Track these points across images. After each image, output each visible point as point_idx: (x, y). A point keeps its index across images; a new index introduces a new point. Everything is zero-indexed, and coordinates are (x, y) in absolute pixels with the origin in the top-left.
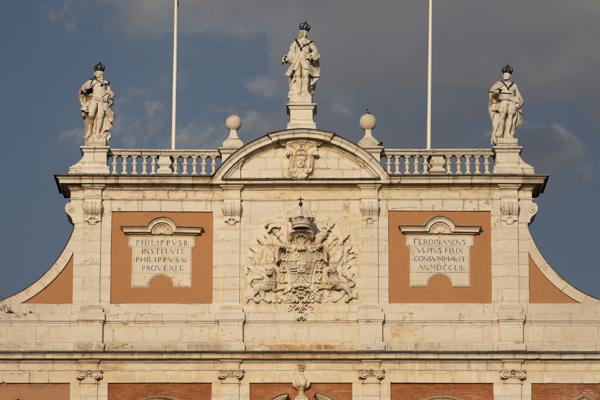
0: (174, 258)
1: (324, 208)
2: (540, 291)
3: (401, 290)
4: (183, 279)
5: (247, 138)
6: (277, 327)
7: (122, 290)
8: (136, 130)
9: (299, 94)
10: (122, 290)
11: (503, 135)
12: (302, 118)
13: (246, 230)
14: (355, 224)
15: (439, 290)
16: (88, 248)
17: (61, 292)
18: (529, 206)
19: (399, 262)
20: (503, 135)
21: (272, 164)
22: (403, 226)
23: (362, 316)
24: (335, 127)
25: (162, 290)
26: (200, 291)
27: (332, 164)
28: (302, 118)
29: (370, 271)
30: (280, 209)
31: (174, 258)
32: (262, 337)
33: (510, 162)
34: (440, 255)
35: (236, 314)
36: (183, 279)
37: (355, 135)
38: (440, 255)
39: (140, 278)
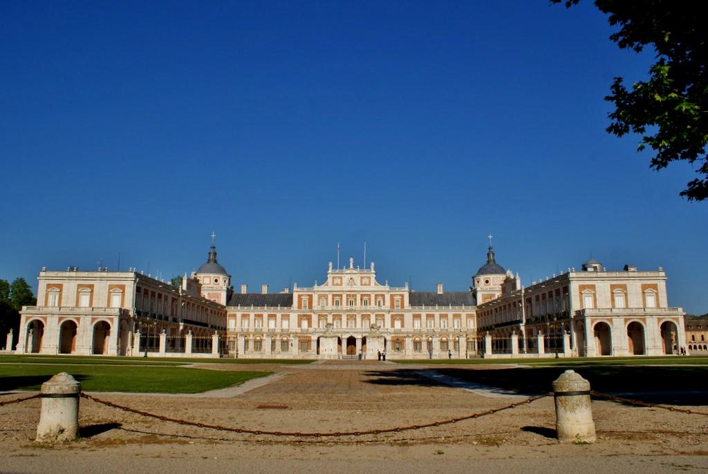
0: (338, 281)
1: (353, 276)
2: (375, 284)
3: (361, 285)
4: (339, 283)
5: (346, 268)
6: (349, 288)
7: (333, 285)
8: (334, 268)
9: (351, 264)
10: (333, 285)
11: (372, 268)
12: (351, 267)
13: (346, 278)
14: (357, 278)
15: (365, 285)
16: (330, 280)
17: (327, 285)
18: (374, 276)
19: (361, 281)
20: (372, 268)
21: (348, 271)
22: (362, 278)
23: (358, 287)
24: (355, 267)
25: (337, 284)
26: (341, 284)
27: (355, 271)
28: (351, 267)
29: (358, 282)
30: (349, 276)
31: (338, 281)
32: (348, 289)
33: (373, 271)
34: (366, 281)
35: (345, 287)
36: (339, 283)
37: (357, 268)
38: (366, 281)
39: (335, 283)
